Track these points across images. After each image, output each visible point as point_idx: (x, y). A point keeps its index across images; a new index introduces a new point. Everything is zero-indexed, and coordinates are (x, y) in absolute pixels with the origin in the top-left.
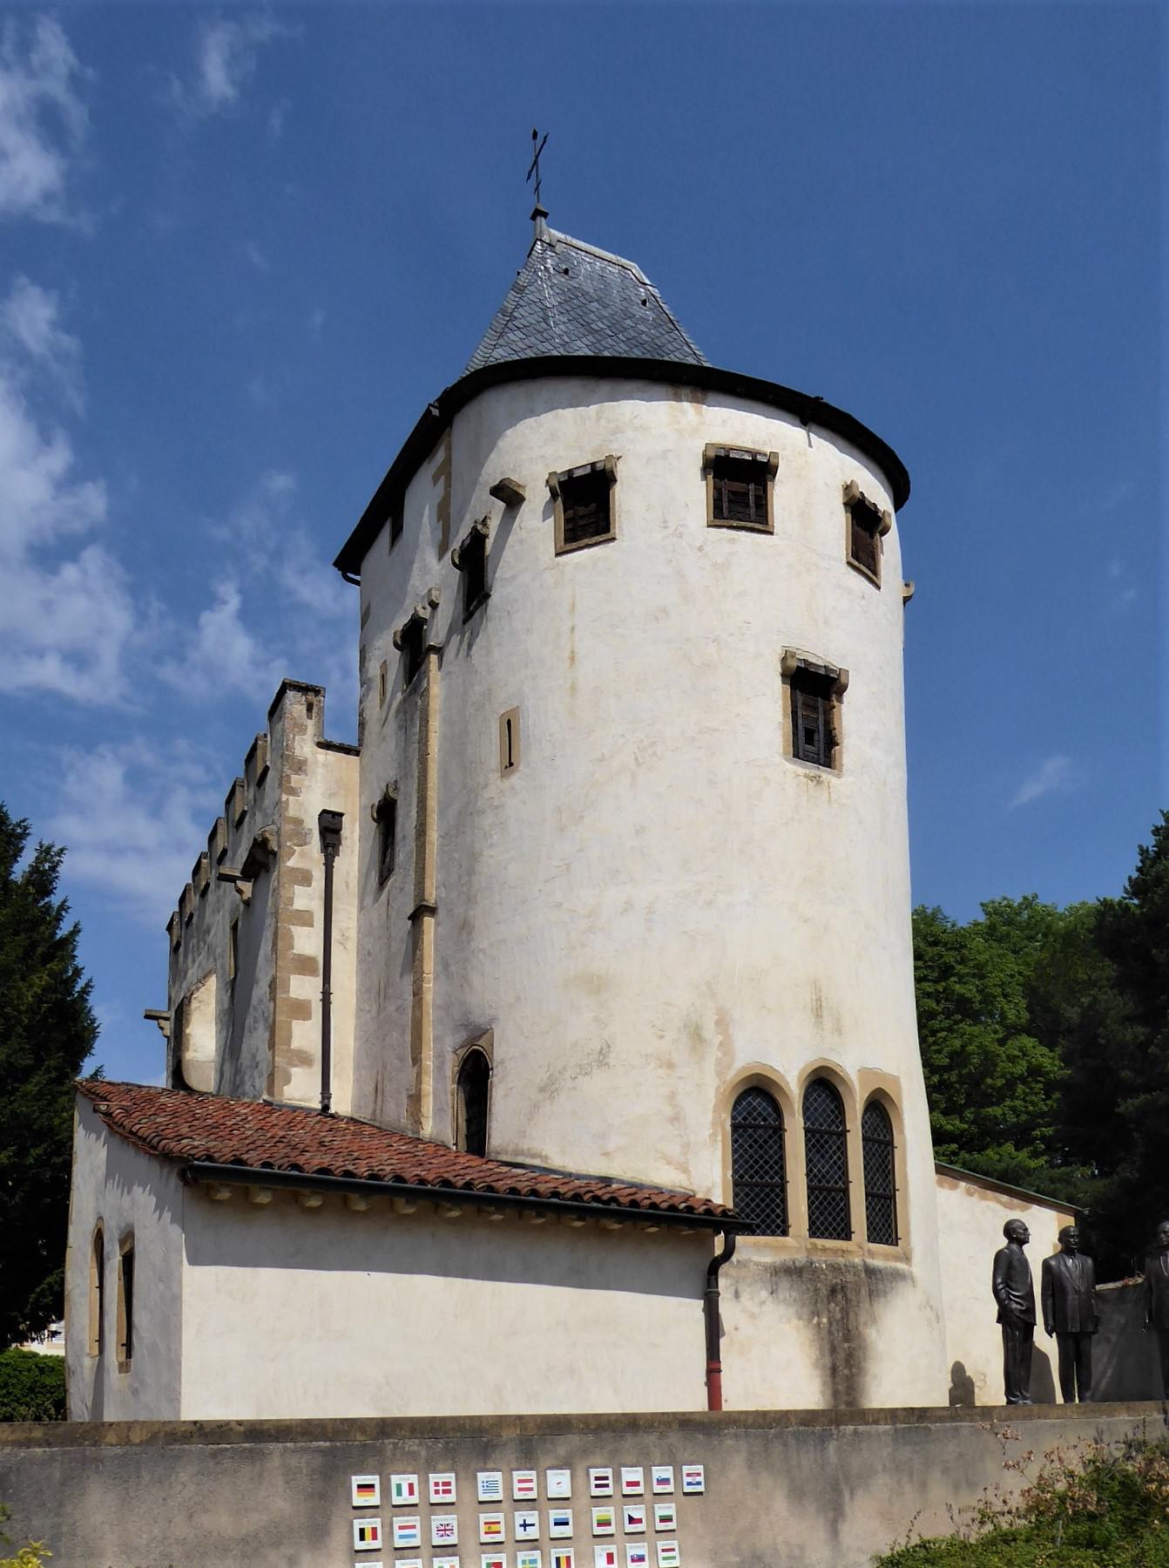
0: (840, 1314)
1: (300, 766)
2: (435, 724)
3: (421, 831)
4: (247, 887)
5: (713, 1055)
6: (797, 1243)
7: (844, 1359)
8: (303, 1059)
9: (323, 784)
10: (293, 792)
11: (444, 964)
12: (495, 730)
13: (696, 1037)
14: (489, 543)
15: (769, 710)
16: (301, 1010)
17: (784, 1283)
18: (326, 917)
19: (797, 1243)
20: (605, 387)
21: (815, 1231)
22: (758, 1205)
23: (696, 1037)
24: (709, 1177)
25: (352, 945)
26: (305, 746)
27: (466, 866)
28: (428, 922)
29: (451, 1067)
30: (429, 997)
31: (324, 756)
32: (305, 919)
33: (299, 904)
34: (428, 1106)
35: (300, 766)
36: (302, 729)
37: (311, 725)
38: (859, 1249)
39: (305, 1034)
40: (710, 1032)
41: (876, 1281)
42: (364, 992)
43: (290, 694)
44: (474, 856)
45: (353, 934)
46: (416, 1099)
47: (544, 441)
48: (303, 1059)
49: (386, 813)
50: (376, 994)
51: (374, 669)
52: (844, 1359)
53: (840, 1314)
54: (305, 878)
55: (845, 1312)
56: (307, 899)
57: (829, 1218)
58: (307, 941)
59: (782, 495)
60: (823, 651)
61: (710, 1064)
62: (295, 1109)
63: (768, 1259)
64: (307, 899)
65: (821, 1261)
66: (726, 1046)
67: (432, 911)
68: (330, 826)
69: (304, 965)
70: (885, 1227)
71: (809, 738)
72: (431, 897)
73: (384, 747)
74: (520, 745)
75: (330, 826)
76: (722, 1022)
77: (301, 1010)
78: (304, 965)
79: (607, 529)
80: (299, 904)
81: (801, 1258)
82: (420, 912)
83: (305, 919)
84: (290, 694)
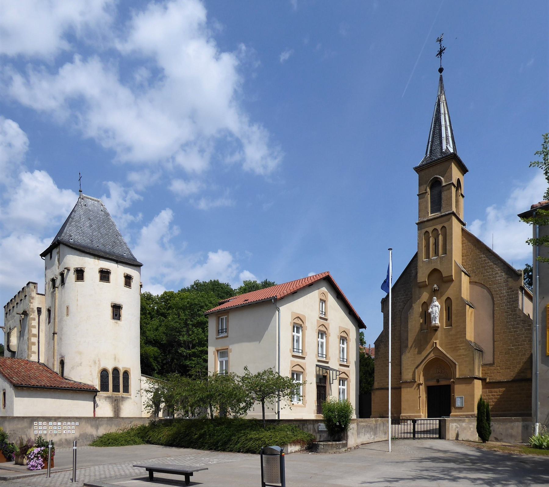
0: (116, 404)
1: (33, 298)
2: (57, 301)
3: (54, 319)
4: (23, 316)
5: (97, 365)
6: (110, 392)
7: (117, 410)
8: (34, 353)
9: (37, 302)
10: (32, 303)
11: (58, 344)
12: (65, 308)
13: (95, 362)
14: (65, 275)
15: (109, 311)
16: (34, 344)
17: (107, 399)
18: (38, 327)
19: (110, 392)
20: (83, 254)
21: (113, 391)
22: (104, 387)
23: (95, 362)
24: (96, 384)
25: (44, 332)
26: (34, 294)
27: (62, 329)
28: (55, 335)
29: (59, 361)
30: (56, 348)
31: (37, 296)
32: (34, 327)
33: (33, 324)
34: (56, 366)
35: (33, 298)
36: (33, 291)
37: (35, 290)
38: (121, 393)
39: (34, 348)
40: (97, 362)
41: (123, 398)
42: (46, 341)
43: (31, 284)
44: (62, 328)
45: (44, 330)
46: (54, 365)
47: (74, 261)
48: (34, 353)
49: (49, 311)
50: (48, 344)
51: (47, 281)
52: (117, 410)
53: (116, 404)
54: (34, 319)
55: (117, 403)
56: (35, 323)
57: (116, 389)
58: (35, 331)
59: (112, 277)
60: (118, 302)
61: (97, 367)
62: (33, 362)
63: (105, 395)
64: (35, 323)
65: (114, 396)
66: (100, 364)
67: (56, 334)
68: (39, 310)
69: (34, 335)
70: (126, 389)
71: (116, 315)
72: (56, 331)
73: (49, 298)
74: (69, 312)
75: (39, 310)
76: (99, 361)
77: (34, 344)
78: (34, 335)
79: (83, 279)
80: (33, 324)
81: (111, 395)
82: (54, 334)
83: (34, 327)
84: (31, 284)
